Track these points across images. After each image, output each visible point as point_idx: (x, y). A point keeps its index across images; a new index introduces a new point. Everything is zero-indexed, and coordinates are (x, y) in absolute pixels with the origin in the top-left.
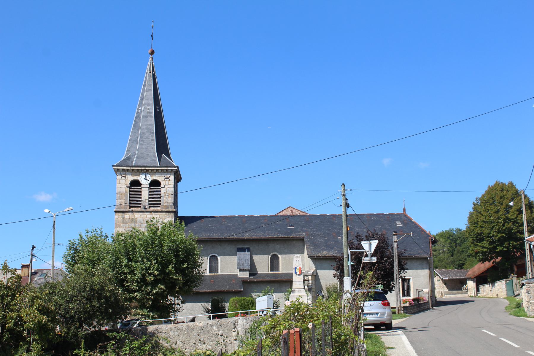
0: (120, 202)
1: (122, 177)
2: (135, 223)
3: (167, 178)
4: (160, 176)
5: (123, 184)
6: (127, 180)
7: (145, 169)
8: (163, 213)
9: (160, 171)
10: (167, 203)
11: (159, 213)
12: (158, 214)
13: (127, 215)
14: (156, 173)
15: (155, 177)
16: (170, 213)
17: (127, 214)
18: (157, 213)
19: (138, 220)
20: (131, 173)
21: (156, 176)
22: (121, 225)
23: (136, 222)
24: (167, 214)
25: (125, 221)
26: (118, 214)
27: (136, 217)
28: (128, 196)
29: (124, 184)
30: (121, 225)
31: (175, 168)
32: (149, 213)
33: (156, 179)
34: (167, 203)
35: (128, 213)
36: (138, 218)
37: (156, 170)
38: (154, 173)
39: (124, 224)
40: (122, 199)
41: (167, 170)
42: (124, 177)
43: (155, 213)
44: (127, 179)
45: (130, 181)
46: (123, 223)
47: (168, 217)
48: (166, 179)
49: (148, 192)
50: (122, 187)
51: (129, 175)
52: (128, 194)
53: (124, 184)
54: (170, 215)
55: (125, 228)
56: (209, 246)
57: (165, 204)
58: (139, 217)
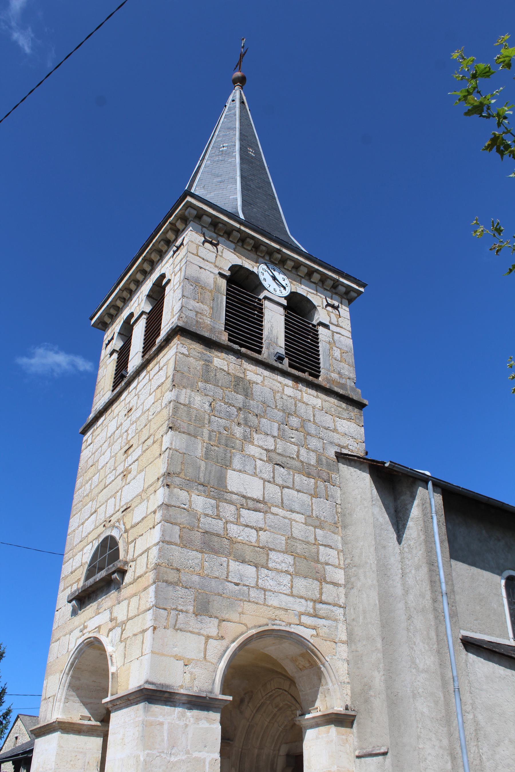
0: (197, 310)
1: (206, 241)
2: (246, 396)
3: (333, 306)
4: (315, 292)
5: (208, 261)
6: (221, 256)
7: (279, 251)
8: (333, 400)
9: (316, 277)
10: (339, 373)
11: (319, 394)
12: (317, 397)
13: (218, 357)
14: (303, 280)
15: (303, 290)
16: (350, 408)
17: (219, 354)
18: (314, 392)
19: (256, 389)
20: (233, 245)
21: (303, 286)
22: (199, 383)
23: (249, 395)
24: (344, 405)
25: (213, 375)
26: (189, 341)
27: (248, 378)
28: (221, 302)
29: (211, 263)
30: (199, 383)
31: (359, 287)
32: (290, 382)
33: (305, 294)
34: (339, 373)
35: (224, 355)
36: (257, 384)
37: (305, 270)
38: (299, 278)
39: (209, 386)
40: (202, 303)
41: (336, 285)
42: (211, 243)
43: (310, 391)
44: (219, 253)
45: (231, 265)
46: (207, 381)
47: (345, 415)
48: (329, 308)
49: (283, 318)
50: (207, 268)
51: (228, 247)
52: (222, 299)
53: (211, 263)
54: (352, 414)
55: (211, 400)
56: (499, 540)
57: (333, 375)
58: (259, 382)
